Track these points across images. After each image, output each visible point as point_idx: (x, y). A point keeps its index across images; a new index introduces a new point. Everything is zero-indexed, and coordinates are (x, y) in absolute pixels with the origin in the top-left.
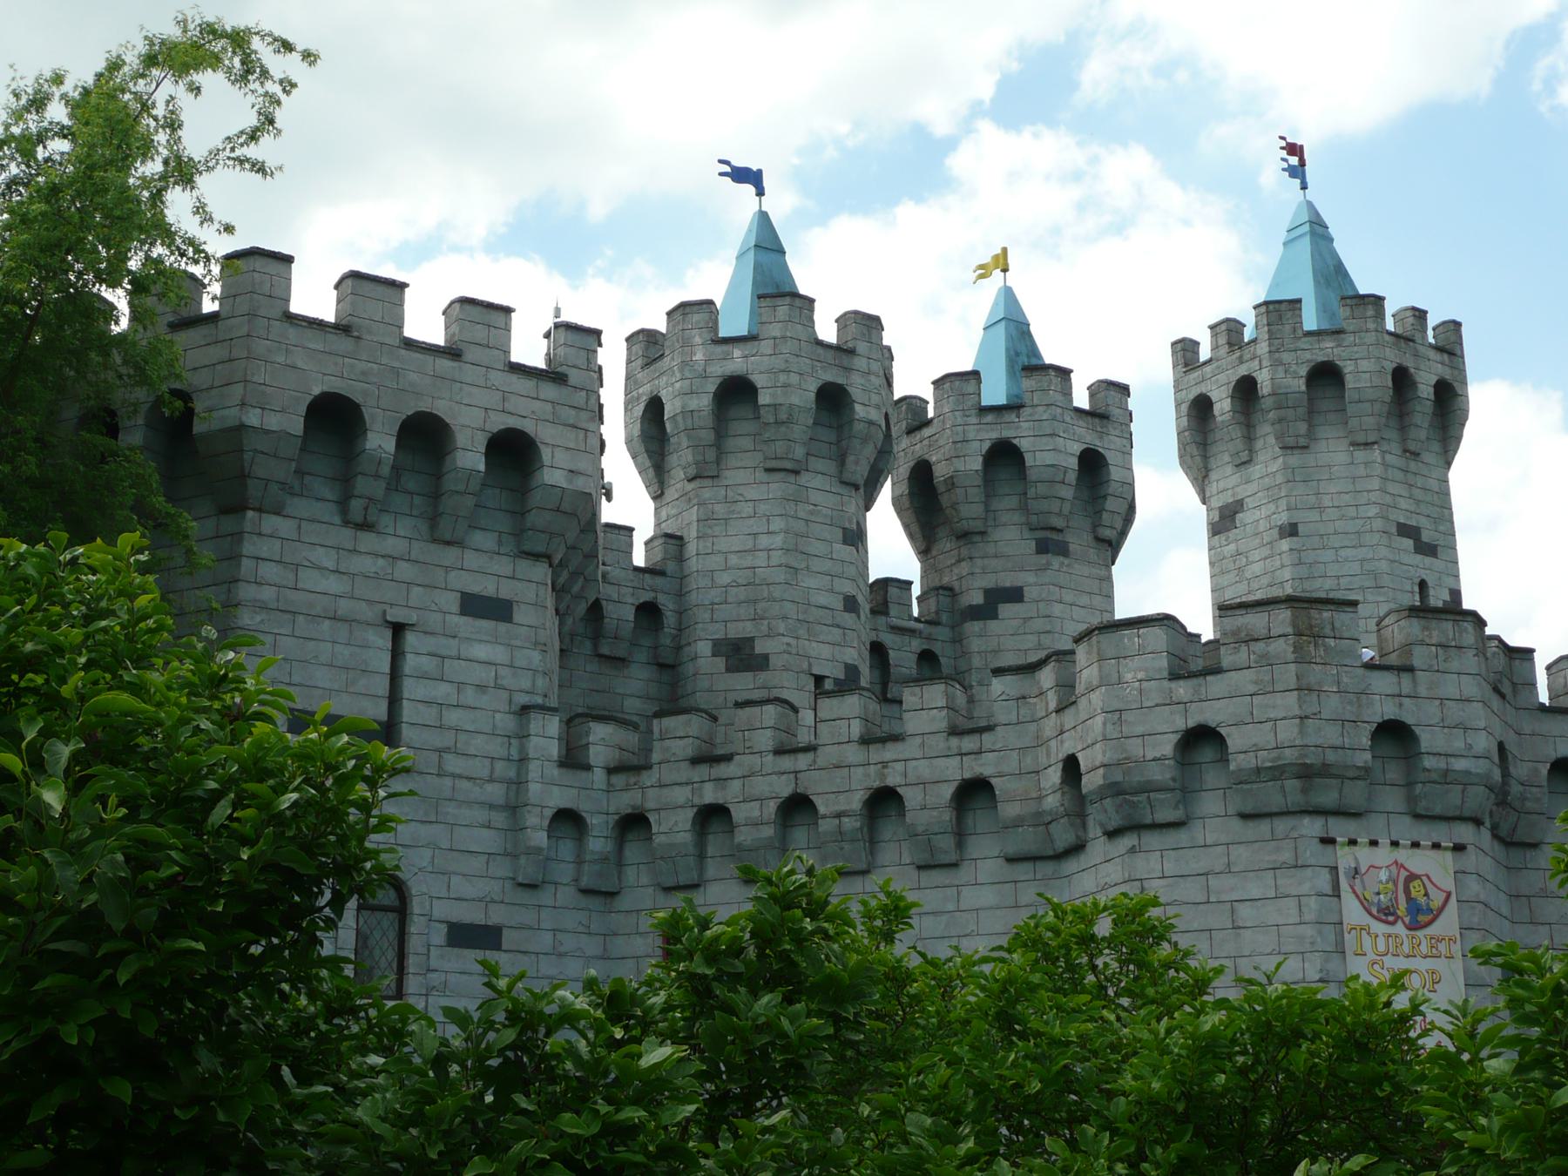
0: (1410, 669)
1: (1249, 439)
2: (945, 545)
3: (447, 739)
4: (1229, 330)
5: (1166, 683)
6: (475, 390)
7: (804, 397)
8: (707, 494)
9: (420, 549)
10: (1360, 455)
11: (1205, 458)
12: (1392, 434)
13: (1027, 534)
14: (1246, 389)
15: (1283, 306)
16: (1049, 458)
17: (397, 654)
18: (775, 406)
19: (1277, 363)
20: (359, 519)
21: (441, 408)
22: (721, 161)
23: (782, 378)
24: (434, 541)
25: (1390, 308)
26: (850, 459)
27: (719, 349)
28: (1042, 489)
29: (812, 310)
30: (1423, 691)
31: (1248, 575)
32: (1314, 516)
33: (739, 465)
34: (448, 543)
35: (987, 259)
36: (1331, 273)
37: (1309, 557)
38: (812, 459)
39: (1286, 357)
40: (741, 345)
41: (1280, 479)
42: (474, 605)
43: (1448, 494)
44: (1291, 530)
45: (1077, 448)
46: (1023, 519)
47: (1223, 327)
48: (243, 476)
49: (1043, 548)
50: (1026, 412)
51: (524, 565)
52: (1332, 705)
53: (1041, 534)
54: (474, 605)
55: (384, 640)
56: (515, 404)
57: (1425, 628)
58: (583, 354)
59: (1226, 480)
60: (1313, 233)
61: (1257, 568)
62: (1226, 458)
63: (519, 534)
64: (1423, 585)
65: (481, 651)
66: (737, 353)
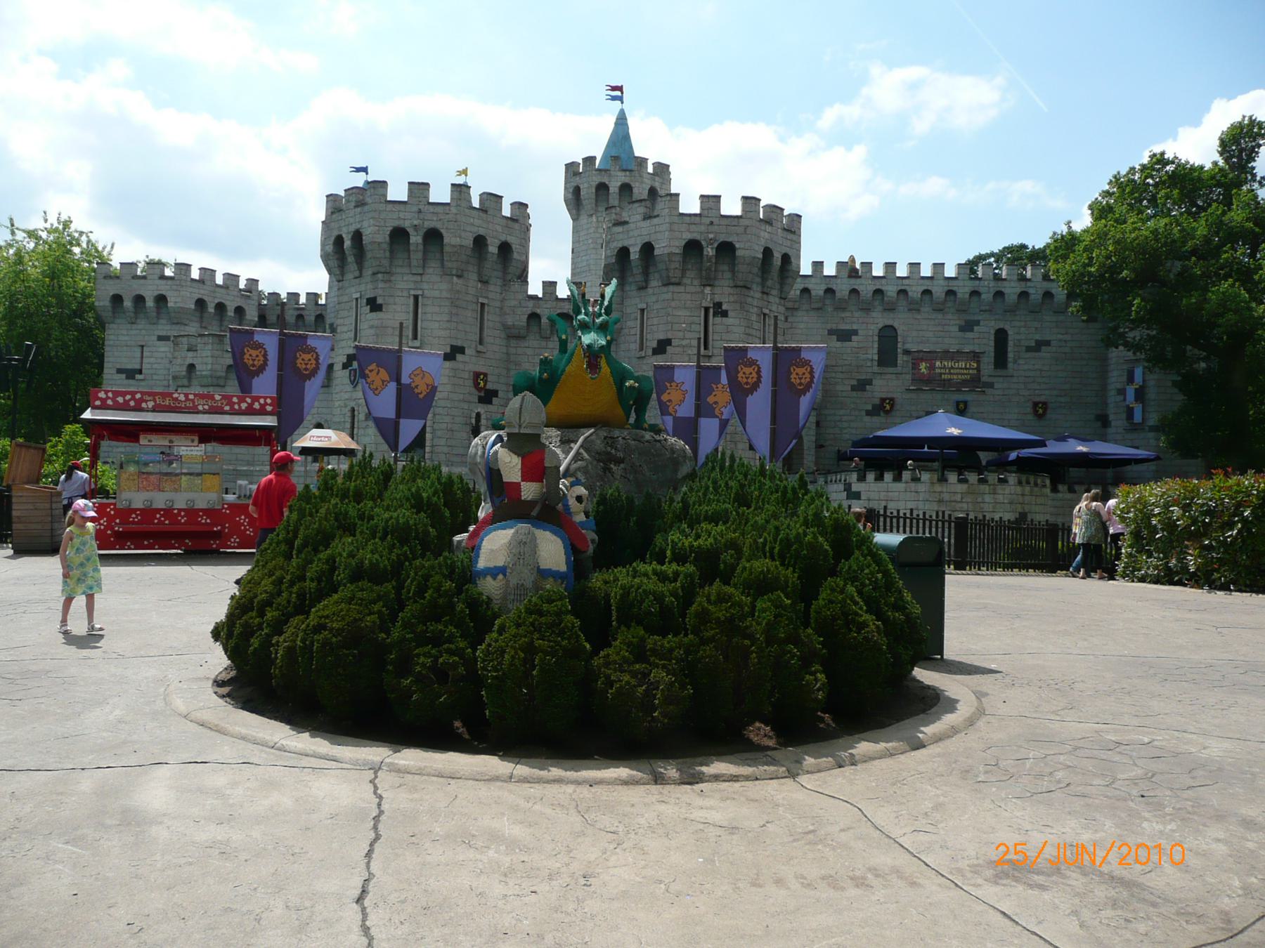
10: (590, 220)
17: (142, 352)
42: (160, 338)
54: (160, 338)
55: (139, 350)
65: (162, 349)
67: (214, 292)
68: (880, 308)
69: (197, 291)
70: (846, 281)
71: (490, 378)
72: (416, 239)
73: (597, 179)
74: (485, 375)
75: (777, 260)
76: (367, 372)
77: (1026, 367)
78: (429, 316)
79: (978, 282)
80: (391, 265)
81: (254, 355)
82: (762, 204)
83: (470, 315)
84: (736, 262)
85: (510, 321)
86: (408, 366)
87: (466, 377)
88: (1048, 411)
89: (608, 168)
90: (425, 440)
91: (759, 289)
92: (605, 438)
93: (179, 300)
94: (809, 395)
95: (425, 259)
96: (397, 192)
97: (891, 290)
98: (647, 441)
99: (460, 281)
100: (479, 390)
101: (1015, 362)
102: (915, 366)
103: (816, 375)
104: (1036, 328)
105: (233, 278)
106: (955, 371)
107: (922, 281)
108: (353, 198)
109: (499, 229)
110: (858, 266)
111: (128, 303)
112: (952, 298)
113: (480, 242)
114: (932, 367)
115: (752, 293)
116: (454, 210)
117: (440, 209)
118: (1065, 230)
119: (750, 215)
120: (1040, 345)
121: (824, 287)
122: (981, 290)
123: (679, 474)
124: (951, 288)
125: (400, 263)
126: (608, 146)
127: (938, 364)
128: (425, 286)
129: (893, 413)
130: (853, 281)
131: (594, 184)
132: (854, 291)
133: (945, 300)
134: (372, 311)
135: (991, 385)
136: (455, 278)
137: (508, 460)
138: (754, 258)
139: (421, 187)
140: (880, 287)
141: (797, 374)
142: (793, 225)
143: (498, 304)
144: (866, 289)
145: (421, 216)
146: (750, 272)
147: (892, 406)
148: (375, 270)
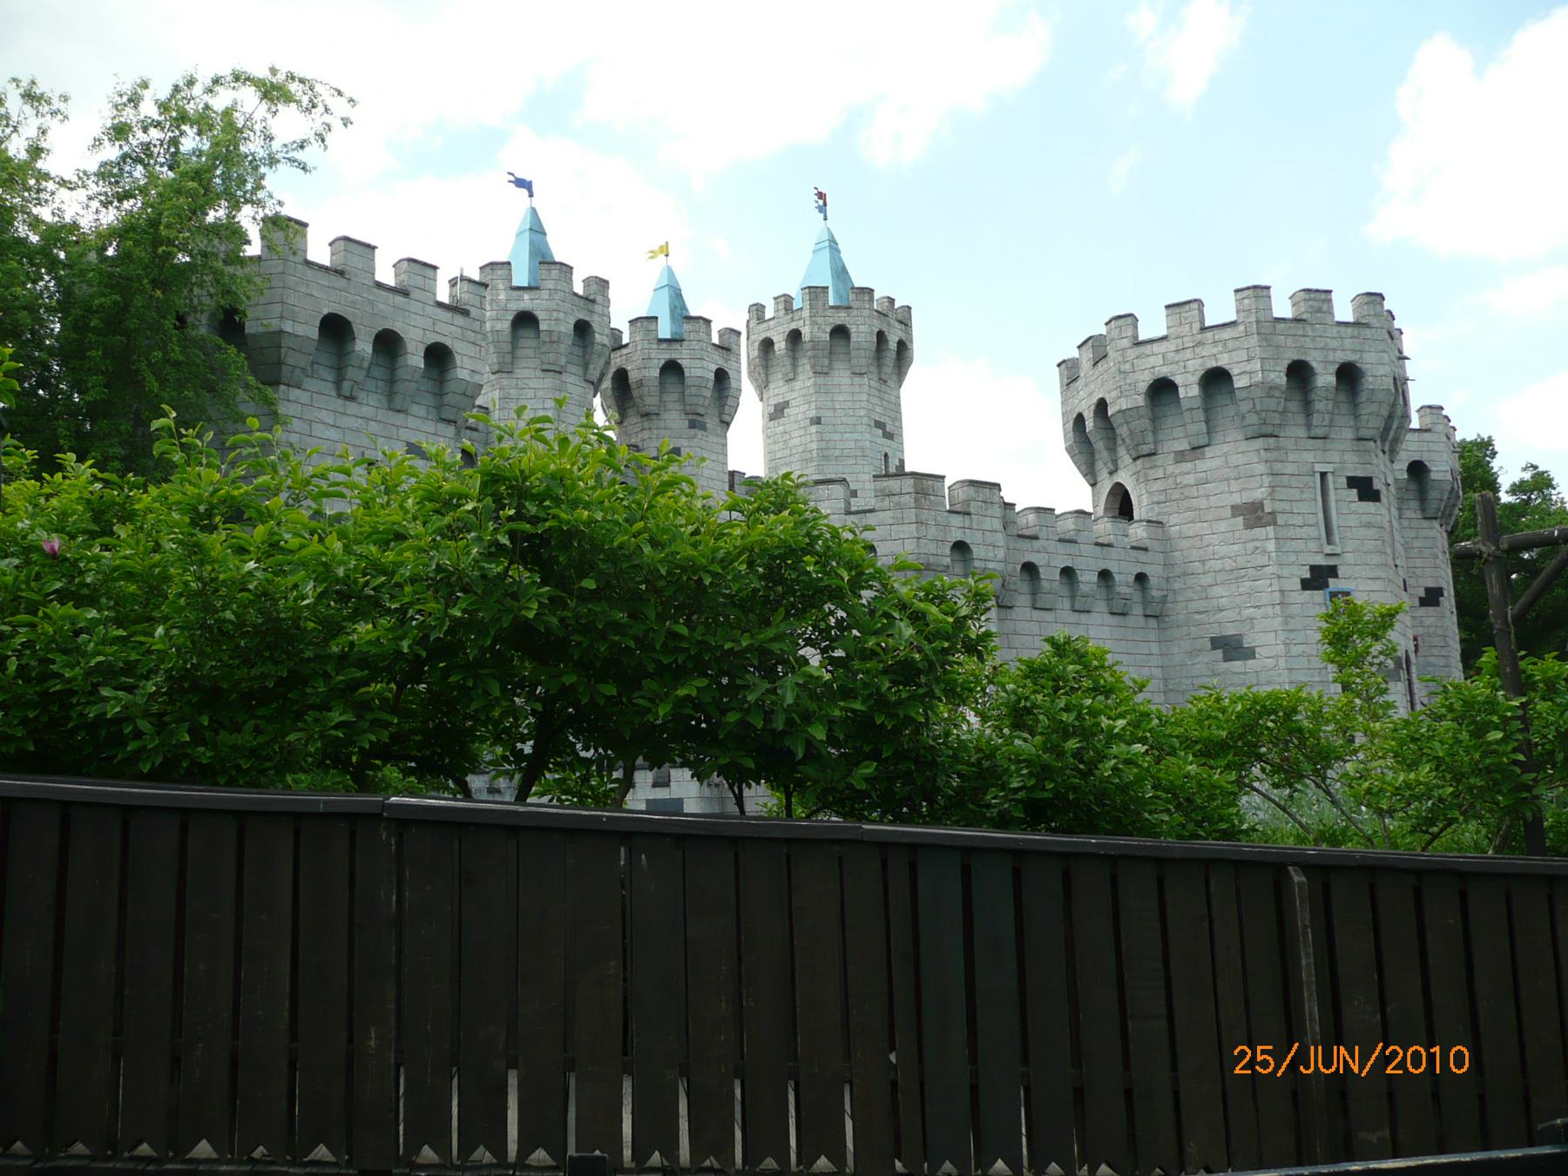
0: (969, 514)
1: (794, 366)
2: (633, 420)
4: (785, 301)
5: (843, 517)
6: (418, 317)
7: (568, 327)
8: (505, 382)
9: (382, 414)
10: (857, 380)
11: (767, 375)
12: (874, 369)
13: (683, 417)
14: (795, 337)
15: (819, 290)
16: (699, 373)
18: (550, 332)
19: (814, 323)
20: (348, 394)
21: (398, 327)
22: (509, 173)
23: (555, 314)
24: (391, 409)
25: (877, 296)
26: (591, 366)
27: (515, 293)
28: (694, 390)
29: (571, 274)
30: (975, 526)
31: (791, 445)
32: (830, 413)
33: (525, 365)
34: (399, 411)
35: (656, 248)
36: (841, 272)
37: (826, 436)
38: (569, 365)
39: (820, 320)
40: (528, 292)
41: (811, 391)
43: (899, 405)
44: (817, 421)
45: (714, 367)
46: (681, 408)
47: (782, 299)
48: (279, 363)
49: (692, 425)
50: (685, 343)
51: (442, 427)
52: (932, 532)
53: (691, 417)
56: (440, 327)
57: (976, 492)
58: (478, 298)
59: (779, 390)
60: (830, 246)
61: (796, 441)
62: (780, 376)
63: (439, 407)
64: (886, 455)
66: (526, 297)
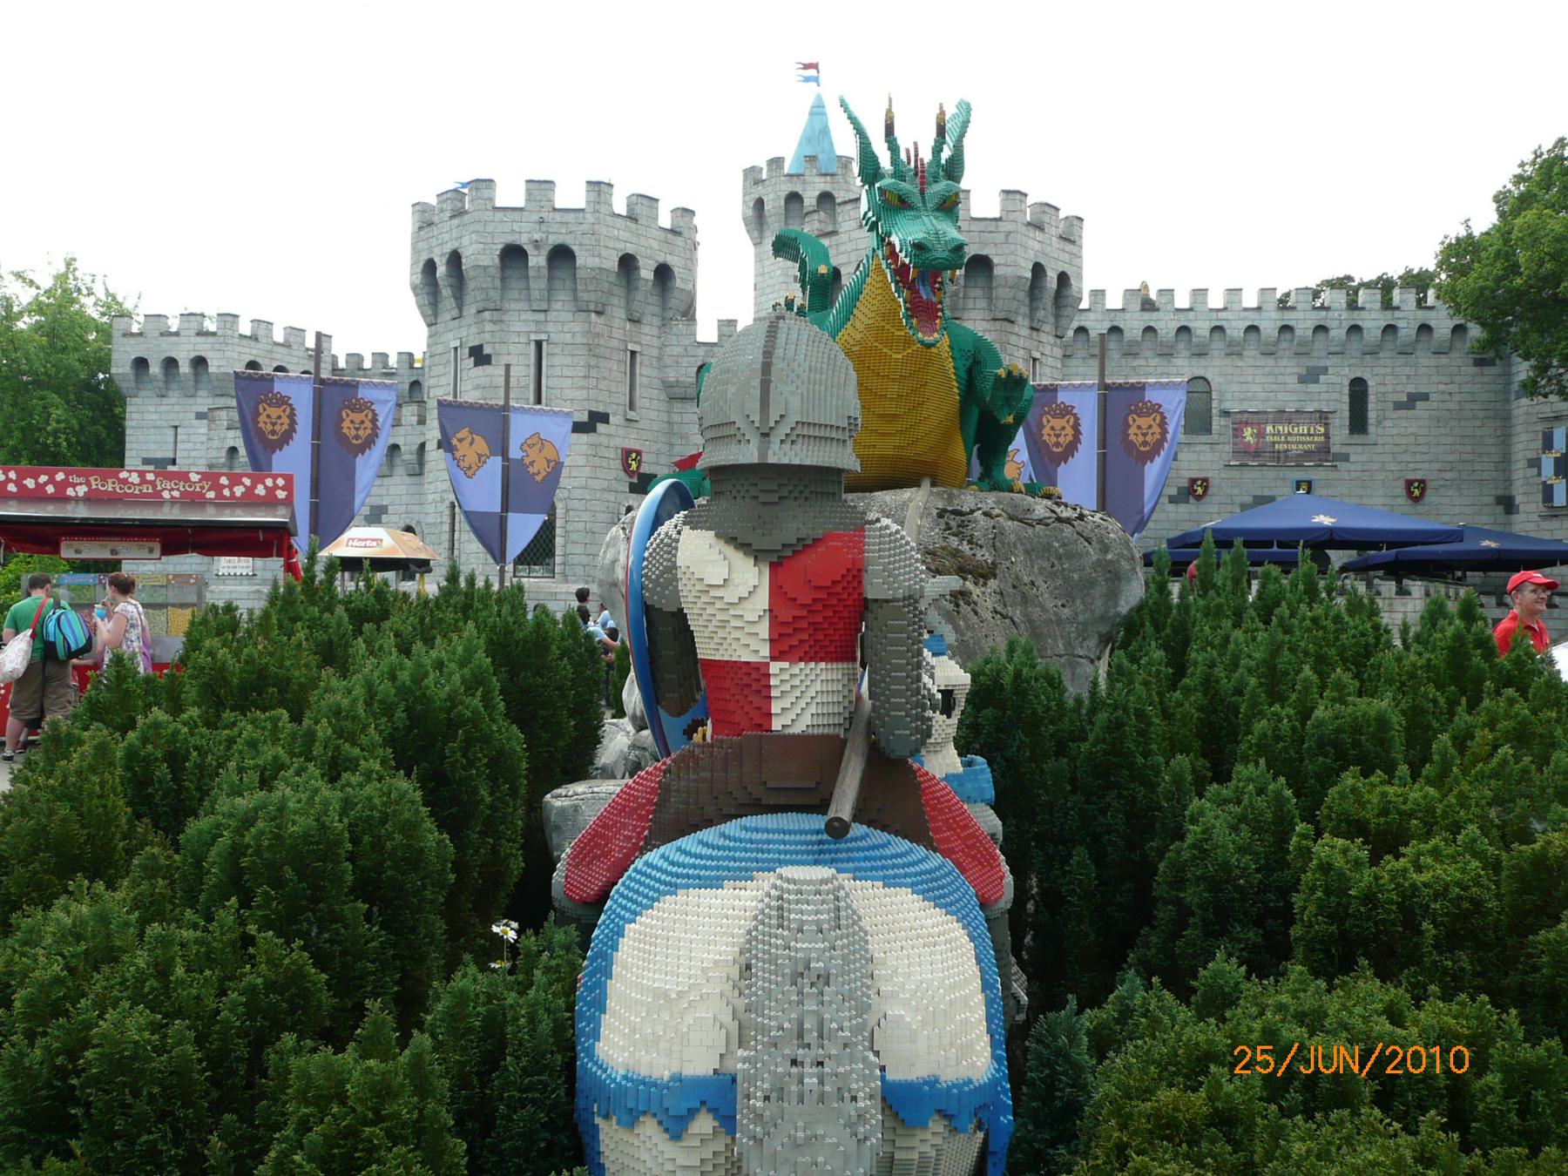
3: (191, 461)
17: (176, 435)
21: (173, 355)
42: (200, 416)
54: (200, 416)
55: (172, 432)
56: (199, 347)
67: (271, 352)
68: (1186, 353)
69: (247, 350)
70: (1138, 315)
71: (645, 457)
72: (537, 260)
73: (786, 188)
74: (639, 453)
75: (1051, 282)
76: (454, 442)
77: (1395, 431)
78: (558, 371)
79: (1324, 313)
80: (502, 299)
81: (274, 416)
82: (1030, 201)
83: (615, 368)
84: (994, 284)
85: (672, 376)
86: (520, 429)
87: (612, 456)
88: (1429, 492)
89: (801, 171)
90: (554, 546)
91: (1027, 323)
92: (941, 515)
93: (223, 363)
94: (1158, 460)
95: (550, 290)
96: (510, 194)
97: (1201, 327)
98: (1040, 522)
99: (601, 320)
100: (630, 474)
101: (1379, 423)
102: (1238, 433)
103: (1171, 429)
104: (1408, 376)
105: (298, 333)
106: (1294, 439)
107: (1246, 313)
108: (448, 206)
109: (655, 245)
110: (1153, 296)
111: (155, 369)
112: (1288, 336)
113: (628, 263)
114: (1261, 435)
115: (1016, 329)
116: (590, 218)
117: (570, 217)
118: (1463, 233)
119: (1012, 216)
120: (1413, 400)
121: (1107, 325)
122: (1328, 324)
123: (1122, 602)
124: (1285, 323)
125: (516, 295)
126: (800, 144)
127: (1269, 429)
128: (551, 327)
129: (1207, 499)
130: (1147, 315)
131: (783, 194)
132: (1149, 330)
133: (1279, 340)
134: (476, 365)
135: (1345, 458)
136: (593, 315)
137: (715, 575)
138: (1020, 277)
139: (543, 186)
140: (1186, 324)
141: (1139, 427)
142: (1071, 233)
143: (655, 352)
144: (1166, 326)
145: (544, 229)
146: (1014, 299)
147: (1206, 489)
148: (481, 306)
